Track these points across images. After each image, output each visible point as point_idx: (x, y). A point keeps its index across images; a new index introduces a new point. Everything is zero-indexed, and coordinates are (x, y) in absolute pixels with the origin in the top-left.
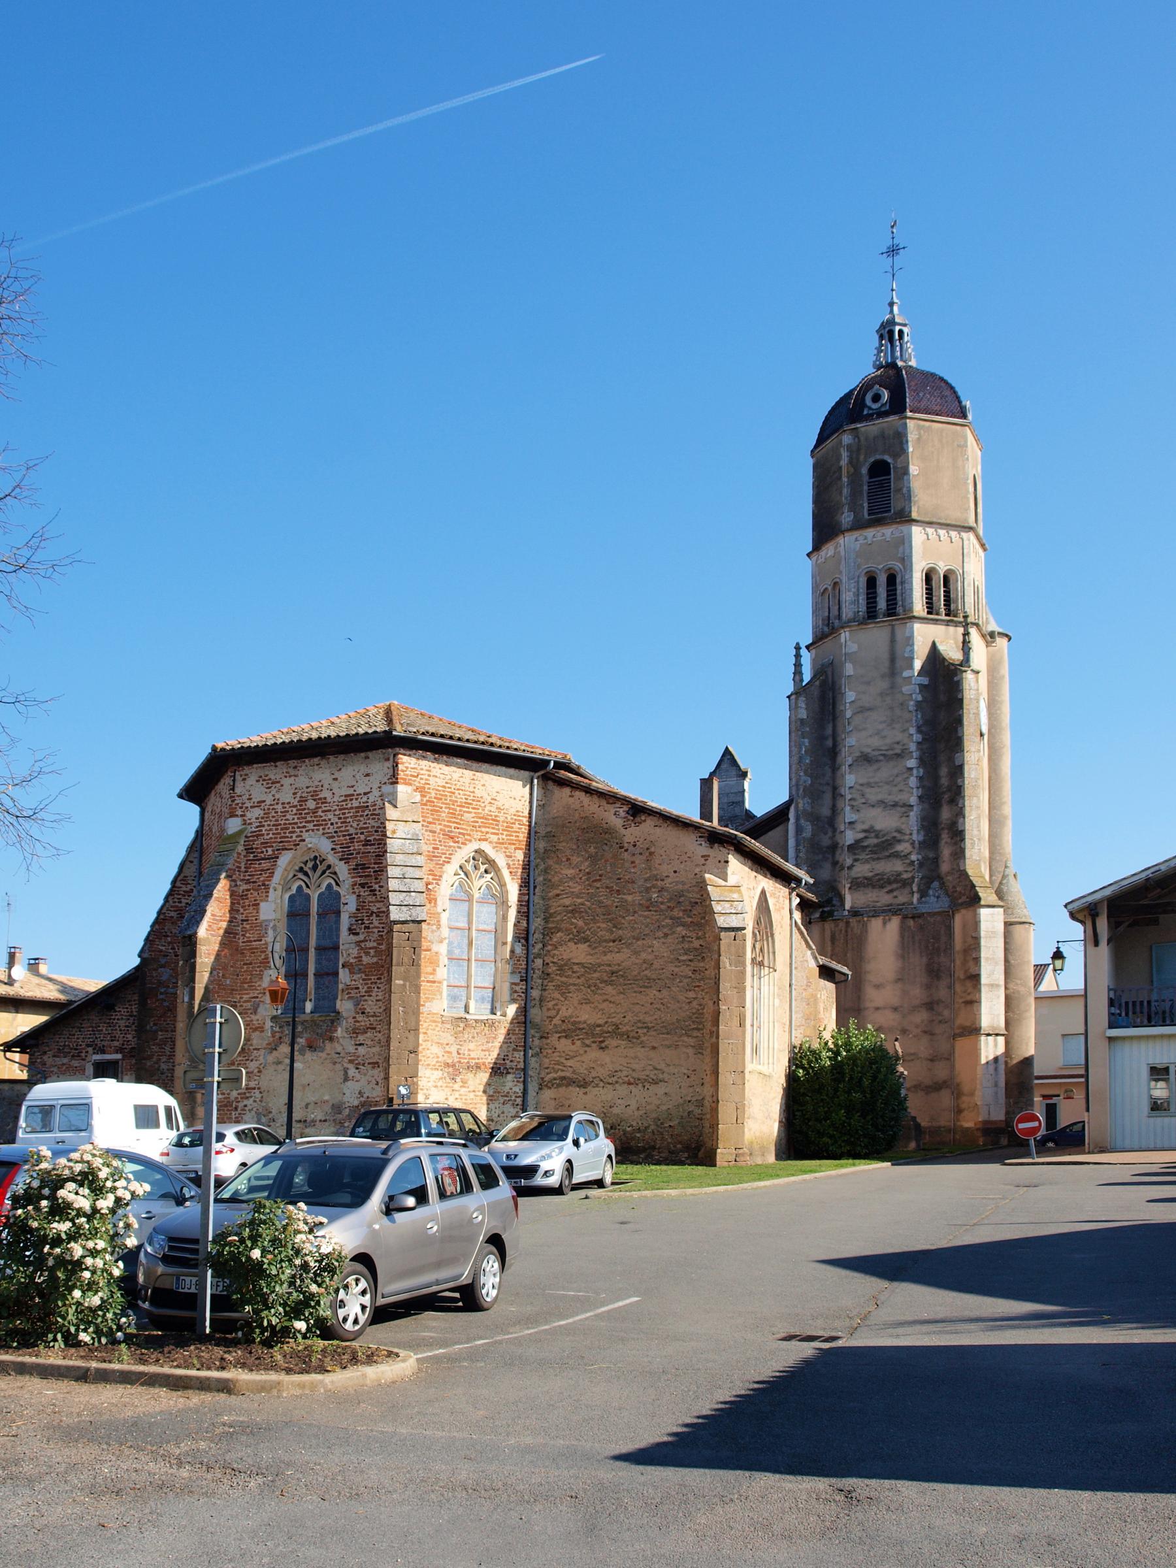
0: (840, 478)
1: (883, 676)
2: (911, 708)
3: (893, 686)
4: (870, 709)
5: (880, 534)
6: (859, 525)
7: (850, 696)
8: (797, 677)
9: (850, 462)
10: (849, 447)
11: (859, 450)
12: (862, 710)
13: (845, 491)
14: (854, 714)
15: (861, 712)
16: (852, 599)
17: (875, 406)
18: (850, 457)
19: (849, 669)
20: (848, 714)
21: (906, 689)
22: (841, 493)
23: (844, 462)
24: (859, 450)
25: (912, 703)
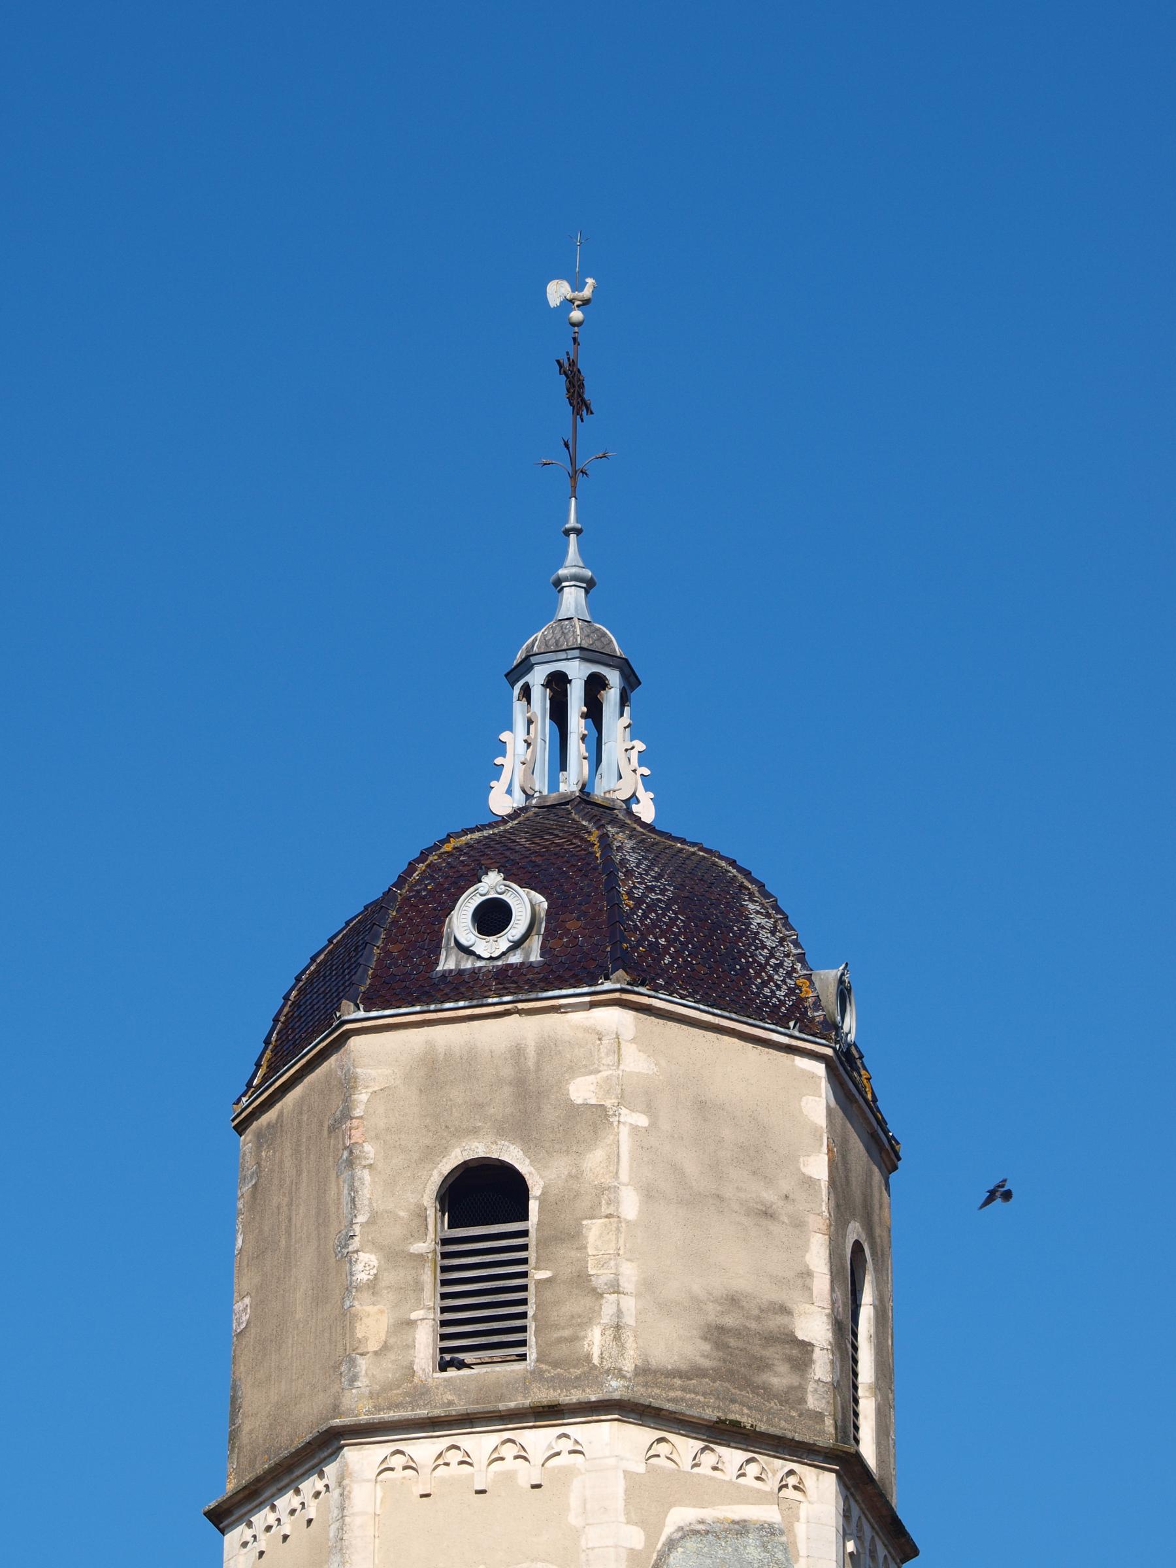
17: (489, 947)
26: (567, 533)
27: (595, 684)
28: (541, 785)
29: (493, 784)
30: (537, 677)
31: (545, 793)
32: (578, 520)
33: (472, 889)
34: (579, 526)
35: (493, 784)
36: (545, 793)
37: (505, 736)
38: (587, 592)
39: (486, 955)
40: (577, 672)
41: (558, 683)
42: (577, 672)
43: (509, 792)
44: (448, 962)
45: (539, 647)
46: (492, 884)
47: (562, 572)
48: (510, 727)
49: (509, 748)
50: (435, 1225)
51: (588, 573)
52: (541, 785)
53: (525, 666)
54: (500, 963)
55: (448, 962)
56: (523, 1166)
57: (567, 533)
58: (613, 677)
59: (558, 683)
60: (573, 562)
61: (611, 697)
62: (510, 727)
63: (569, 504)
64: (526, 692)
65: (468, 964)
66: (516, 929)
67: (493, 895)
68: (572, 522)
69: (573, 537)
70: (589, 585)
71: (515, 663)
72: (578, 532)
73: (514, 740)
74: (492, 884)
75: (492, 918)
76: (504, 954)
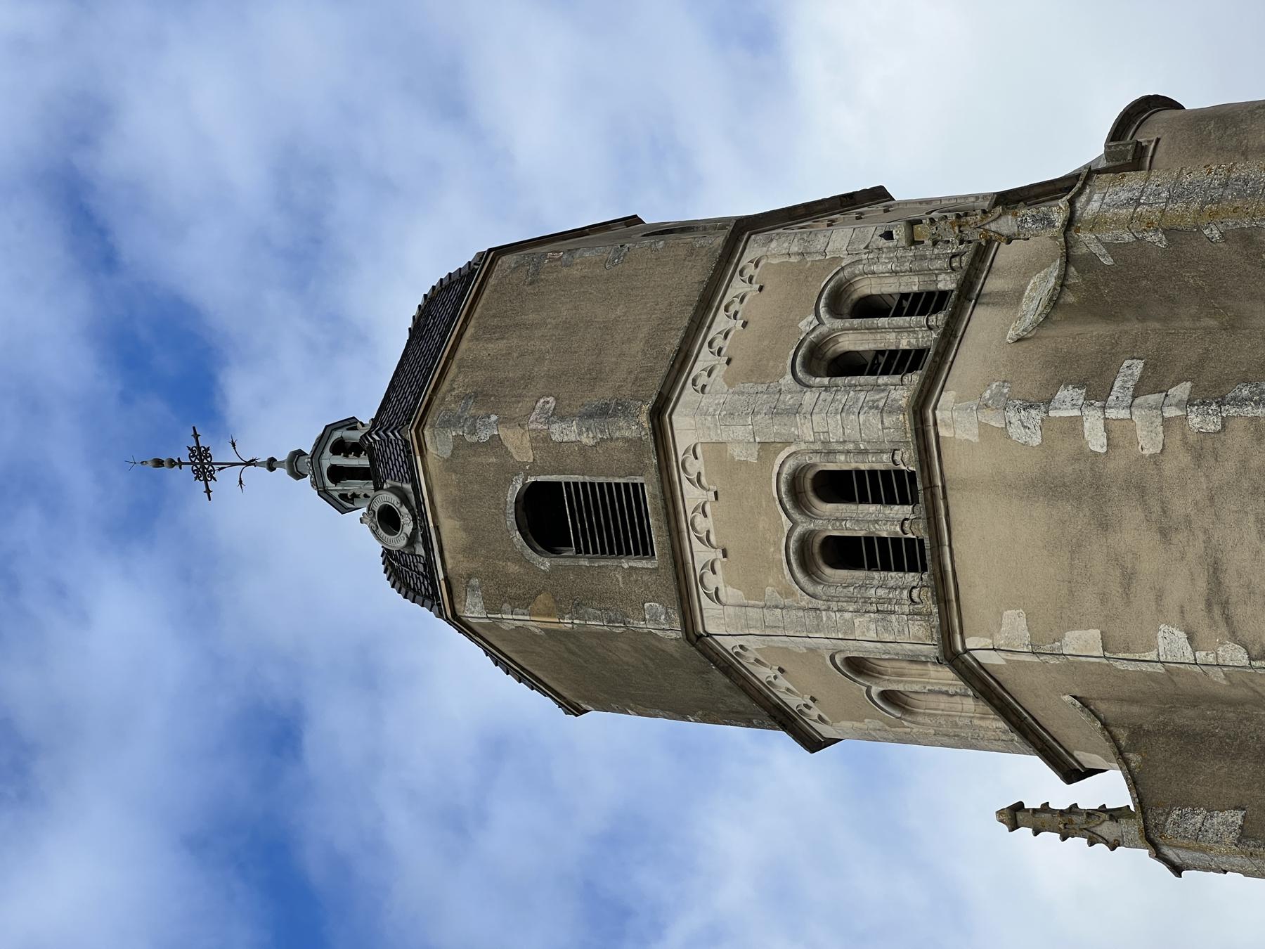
1: (1104, 526)
2: (1213, 424)
3: (1138, 489)
4: (1216, 572)
5: (700, 522)
6: (682, 588)
7: (1171, 644)
8: (1107, 829)
12: (1217, 600)
14: (1234, 637)
15: (1225, 605)
16: (877, 618)
19: (1083, 642)
20: (1235, 656)
21: (1148, 440)
25: (1195, 420)
40: (329, 460)
41: (337, 474)
42: (329, 460)
66: (393, 500)
67: (376, 520)
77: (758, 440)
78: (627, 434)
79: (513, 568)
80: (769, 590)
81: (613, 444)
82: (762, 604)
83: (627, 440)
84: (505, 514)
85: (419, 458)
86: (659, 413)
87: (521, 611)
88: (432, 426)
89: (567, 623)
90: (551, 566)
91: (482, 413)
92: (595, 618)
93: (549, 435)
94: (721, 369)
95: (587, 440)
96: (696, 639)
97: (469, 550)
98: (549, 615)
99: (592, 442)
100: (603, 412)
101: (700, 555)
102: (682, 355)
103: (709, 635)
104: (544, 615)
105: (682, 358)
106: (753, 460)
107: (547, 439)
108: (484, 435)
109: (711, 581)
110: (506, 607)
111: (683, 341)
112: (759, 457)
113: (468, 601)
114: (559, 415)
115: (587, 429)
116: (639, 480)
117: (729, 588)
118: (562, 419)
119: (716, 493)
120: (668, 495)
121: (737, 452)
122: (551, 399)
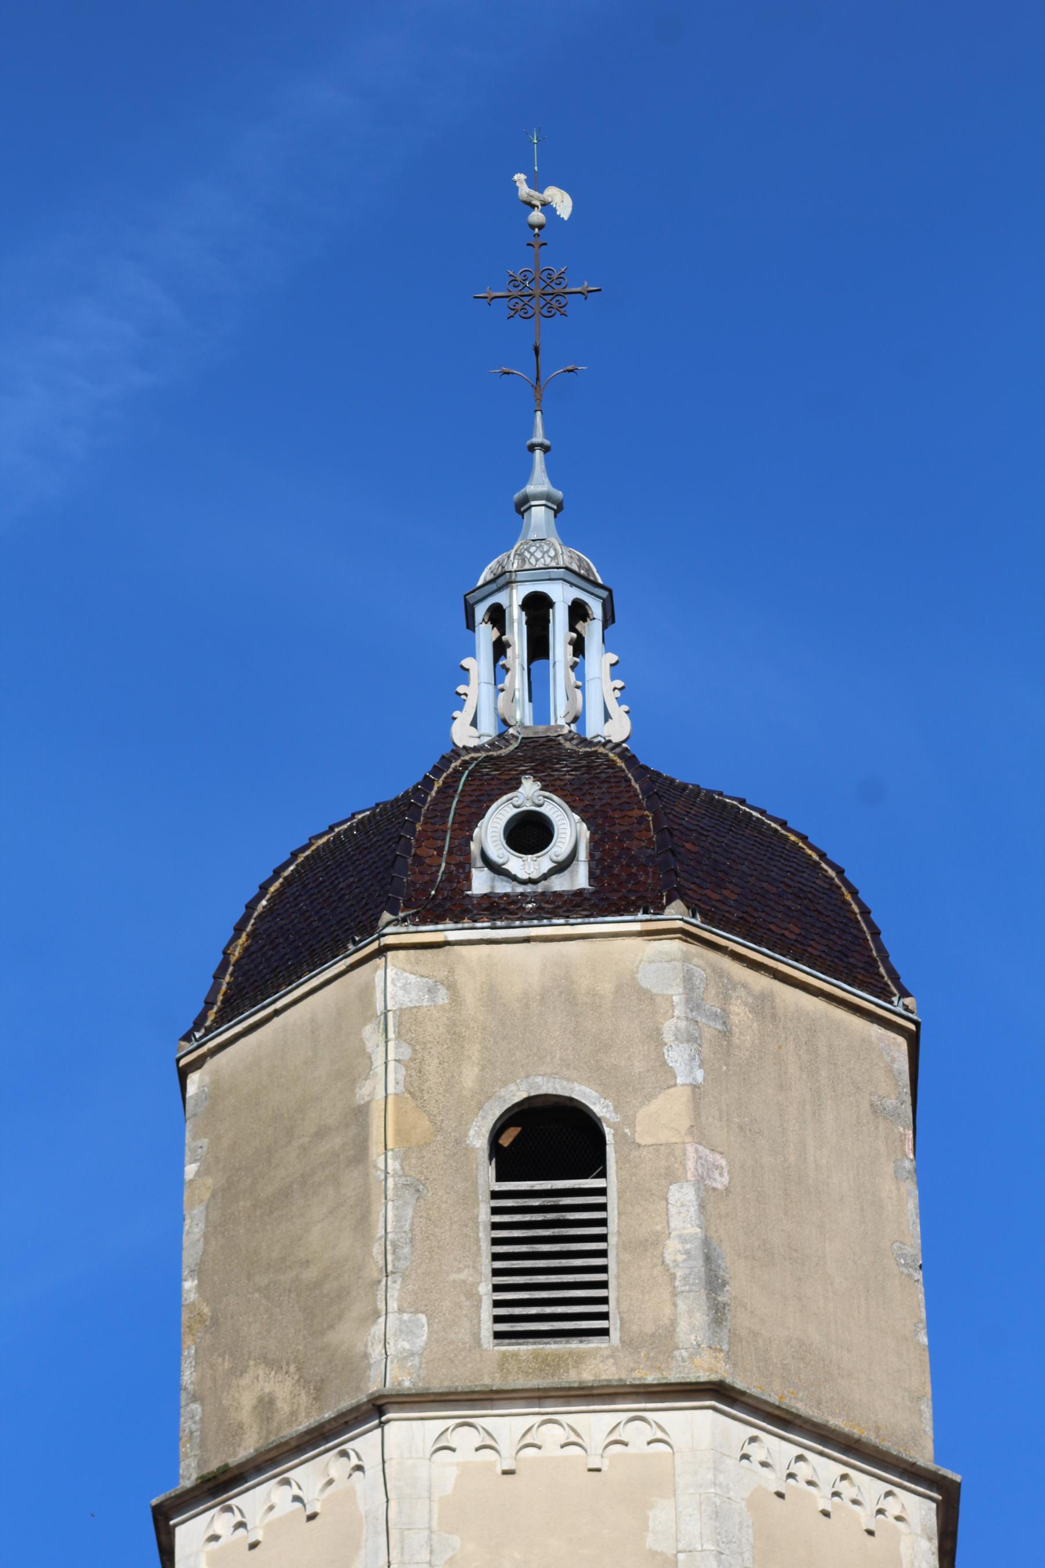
0: (359, 1153)
9: (414, 1091)
10: (408, 1016)
11: (455, 1036)
13: (391, 1216)
18: (415, 1067)
22: (363, 1222)
23: (383, 1083)
24: (455, 1036)
26: (532, 448)
27: (578, 612)
28: (523, 714)
29: (456, 714)
30: (513, 599)
31: (528, 722)
32: (546, 435)
33: (505, 798)
34: (547, 442)
35: (456, 714)
36: (528, 722)
37: (466, 662)
38: (556, 512)
39: (523, 876)
40: (561, 595)
41: (537, 607)
43: (474, 723)
44: (481, 882)
45: (515, 565)
46: (529, 793)
47: (530, 489)
48: (473, 654)
49: (473, 675)
50: (486, 1175)
51: (559, 494)
52: (523, 714)
53: (503, 581)
54: (540, 888)
55: (481, 882)
56: (600, 1108)
57: (532, 448)
58: (596, 608)
59: (537, 607)
60: (539, 483)
61: (593, 631)
62: (473, 654)
63: (534, 418)
64: (497, 616)
65: (503, 887)
66: (559, 848)
67: (529, 807)
68: (539, 438)
69: (538, 453)
70: (558, 508)
71: (480, 582)
72: (546, 449)
73: (479, 665)
74: (529, 793)
75: (529, 834)
76: (545, 877)
77: (681, 1557)
78: (683, 1326)
79: (469, 1077)
80: (456, 1540)
81: (666, 1296)
82: (435, 1524)
83: (674, 1323)
84: (552, 1075)
85: (637, 927)
86: (720, 1393)
87: (401, 1078)
88: (686, 958)
89: (385, 1162)
90: (474, 1150)
91: (705, 1049)
92: (398, 1219)
93: (675, 1180)
94: (773, 1481)
95: (672, 1249)
96: (376, 1409)
97: (491, 995)
98: (398, 1132)
99: (669, 1258)
100: (714, 1282)
101: (507, 1426)
102: (788, 1417)
103: (382, 1425)
104: (397, 1123)
105: (783, 1420)
106: (650, 1542)
107: (672, 1177)
108: (677, 1056)
109: (465, 1439)
110: (406, 1052)
111: (807, 1421)
112: (654, 1554)
113: (412, 978)
114: (707, 1201)
115: (687, 1253)
116: (615, 1334)
117: (453, 1472)
118: (702, 1207)
119: (599, 1470)
120: (595, 1392)
121: (661, 1516)
122: (725, 1180)
